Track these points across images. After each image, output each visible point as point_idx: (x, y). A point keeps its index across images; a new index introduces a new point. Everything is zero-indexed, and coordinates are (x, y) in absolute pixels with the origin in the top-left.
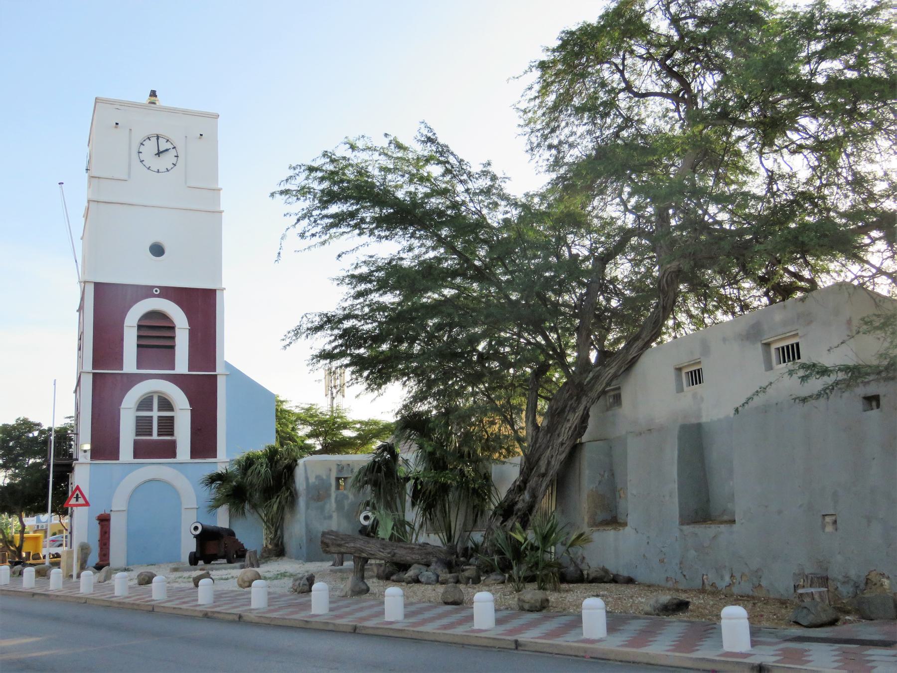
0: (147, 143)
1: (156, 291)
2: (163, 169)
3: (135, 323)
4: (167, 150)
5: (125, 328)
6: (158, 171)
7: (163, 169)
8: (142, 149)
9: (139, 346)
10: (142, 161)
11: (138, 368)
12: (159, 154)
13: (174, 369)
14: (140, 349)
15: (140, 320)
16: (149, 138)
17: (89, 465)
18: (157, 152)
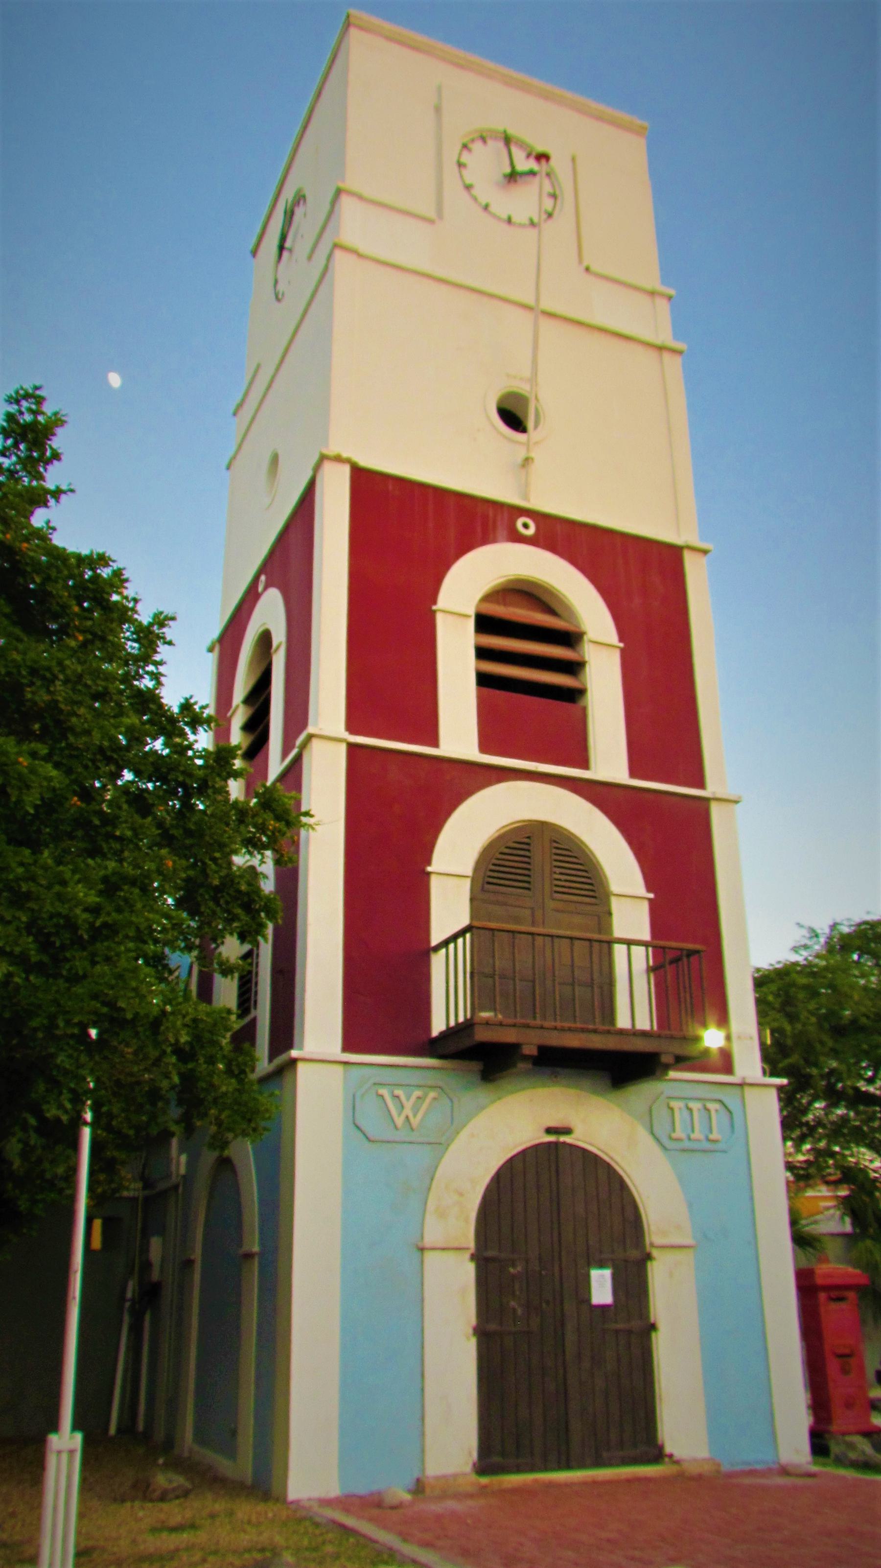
0: (477, 146)
1: (526, 526)
2: (520, 217)
3: (472, 612)
4: (532, 173)
5: (440, 619)
6: (509, 221)
7: (520, 217)
8: (466, 158)
9: (484, 680)
10: (468, 188)
11: (485, 746)
12: (513, 177)
13: (584, 764)
14: (486, 691)
15: (489, 598)
16: (483, 140)
17: (340, 1068)
18: (508, 170)
